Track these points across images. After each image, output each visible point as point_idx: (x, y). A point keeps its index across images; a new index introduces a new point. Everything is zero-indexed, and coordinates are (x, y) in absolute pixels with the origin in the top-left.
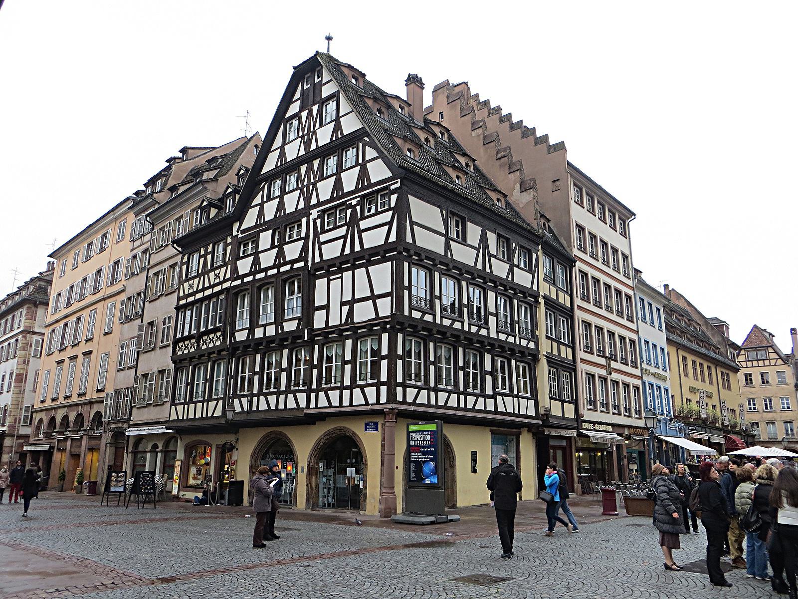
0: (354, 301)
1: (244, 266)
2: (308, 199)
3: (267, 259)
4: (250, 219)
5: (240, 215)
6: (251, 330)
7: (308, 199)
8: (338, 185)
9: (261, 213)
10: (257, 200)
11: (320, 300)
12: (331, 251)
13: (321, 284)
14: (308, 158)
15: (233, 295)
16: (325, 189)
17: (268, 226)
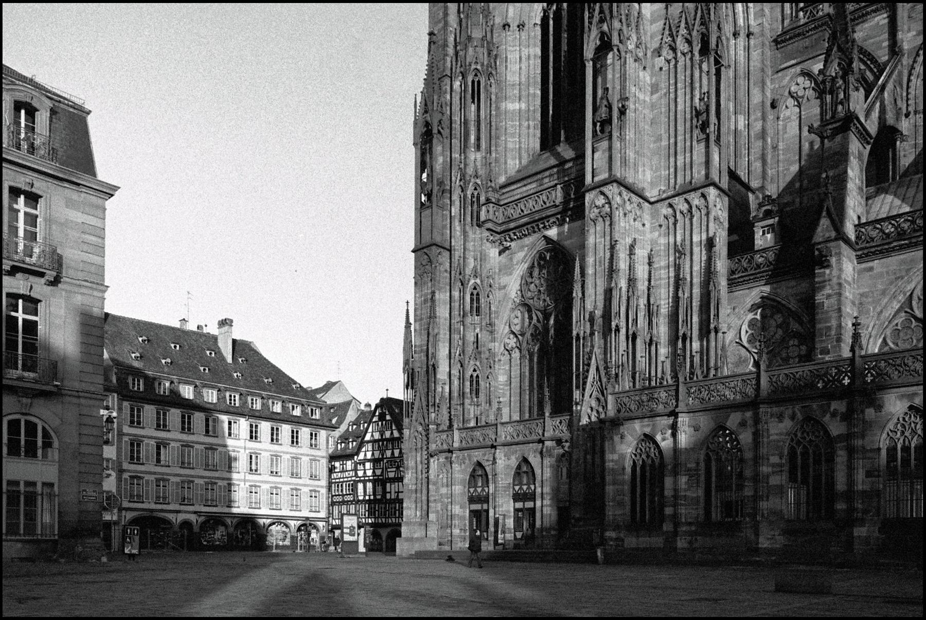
0: (398, 492)
1: (360, 473)
2: (383, 455)
3: (369, 473)
4: (361, 456)
5: (357, 454)
6: (364, 496)
7: (383, 455)
8: (393, 453)
9: (365, 455)
10: (364, 449)
11: (388, 490)
12: (392, 475)
13: (388, 485)
14: (382, 440)
15: (356, 482)
16: (389, 453)
17: (369, 461)
